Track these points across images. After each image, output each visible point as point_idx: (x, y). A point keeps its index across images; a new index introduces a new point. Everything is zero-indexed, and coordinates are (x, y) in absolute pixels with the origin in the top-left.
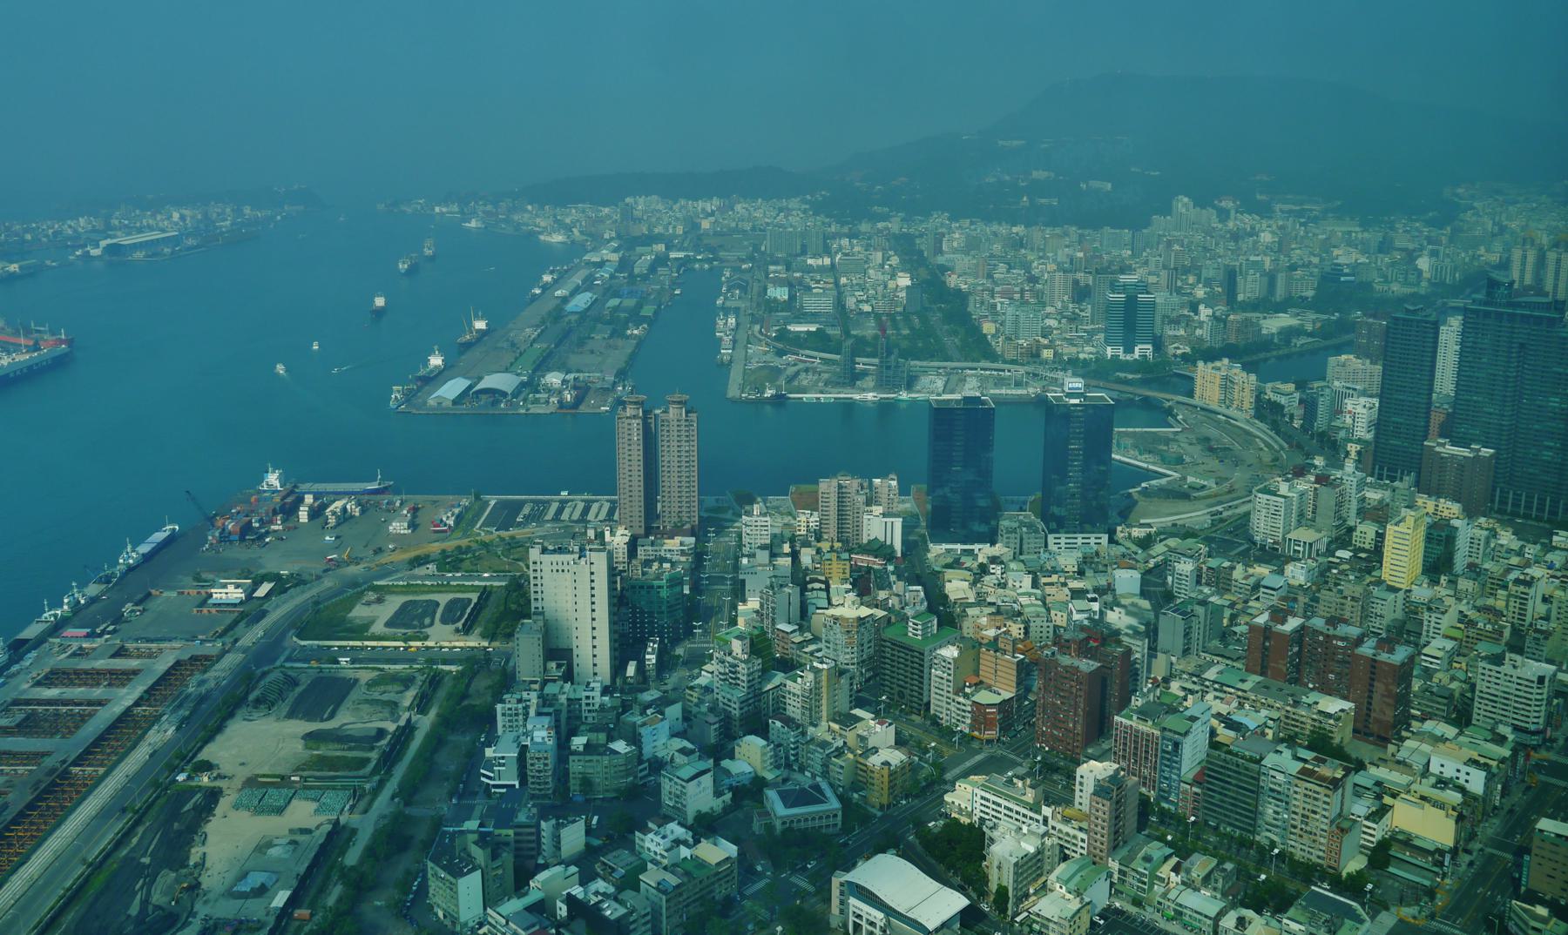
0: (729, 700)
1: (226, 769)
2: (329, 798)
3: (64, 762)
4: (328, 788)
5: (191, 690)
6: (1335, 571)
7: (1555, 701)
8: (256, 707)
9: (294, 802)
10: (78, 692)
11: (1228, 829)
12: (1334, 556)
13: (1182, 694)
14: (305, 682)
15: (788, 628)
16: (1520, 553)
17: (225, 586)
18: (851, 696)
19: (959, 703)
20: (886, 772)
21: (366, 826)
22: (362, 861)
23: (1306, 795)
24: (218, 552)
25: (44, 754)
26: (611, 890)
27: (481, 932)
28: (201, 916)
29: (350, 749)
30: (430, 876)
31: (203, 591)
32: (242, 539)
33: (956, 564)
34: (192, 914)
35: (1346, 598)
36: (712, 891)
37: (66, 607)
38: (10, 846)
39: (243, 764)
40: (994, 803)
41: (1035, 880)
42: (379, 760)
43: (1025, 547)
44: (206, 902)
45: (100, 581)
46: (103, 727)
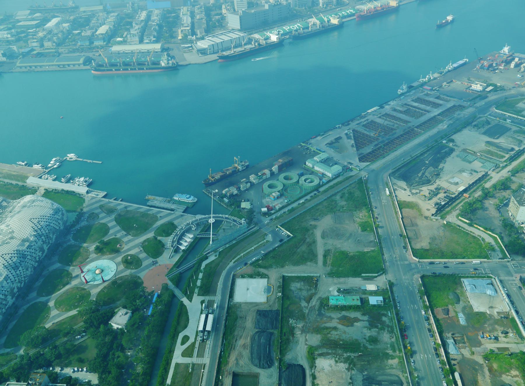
1: (458, 144)
2: (487, 164)
3: (413, 126)
4: (488, 161)
5: (455, 116)
8: (474, 127)
9: (476, 161)
10: (423, 106)
14: (493, 124)
17: (477, 84)
21: (496, 177)
22: (490, 188)
24: (478, 72)
25: (410, 122)
27: (522, 226)
28: (437, 184)
29: (500, 151)
30: (511, 201)
31: (469, 84)
32: (488, 69)
34: (435, 182)
37: (427, 79)
38: (394, 145)
39: (463, 144)
42: (508, 158)
44: (440, 180)
45: (438, 73)
46: (427, 119)
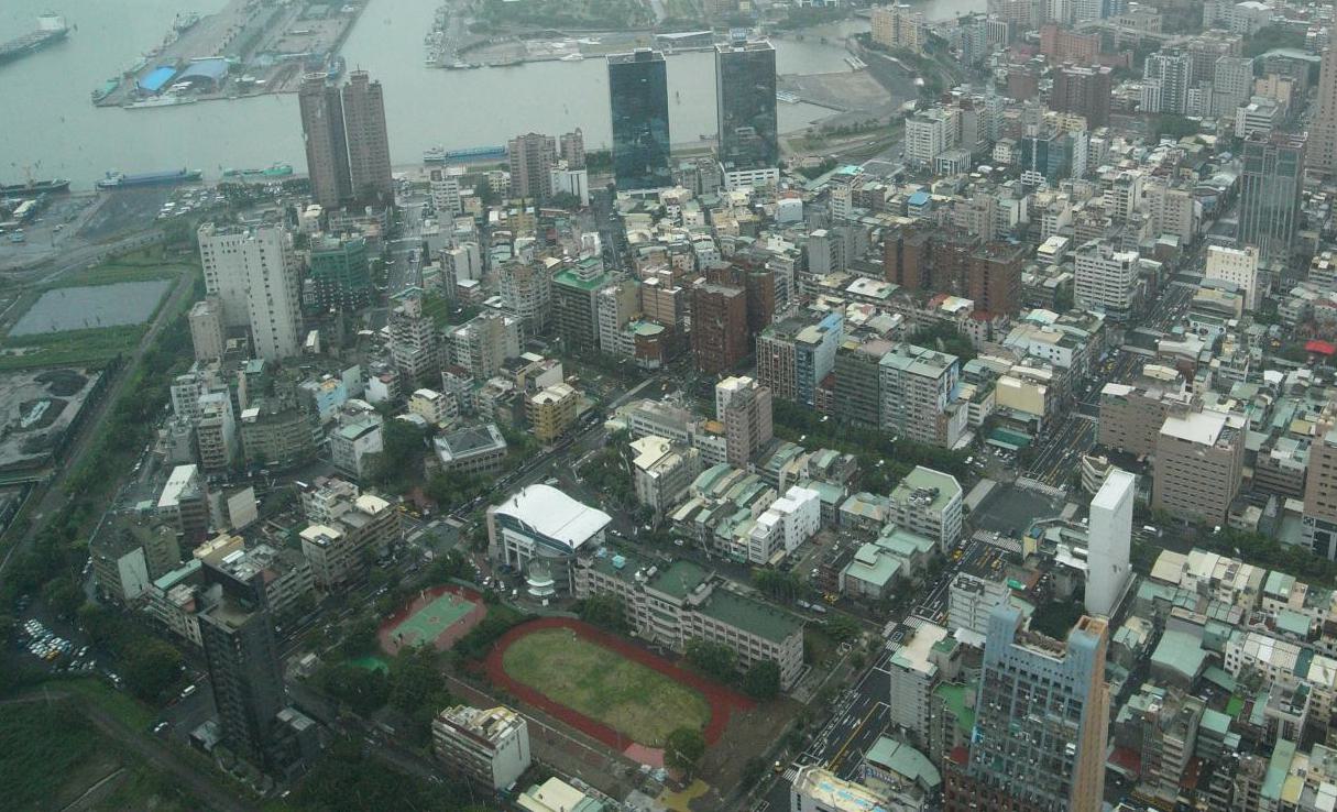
0: (404, 358)
6: (972, 185)
7: (1140, 281)
11: (860, 425)
12: (976, 172)
13: (827, 308)
15: (467, 283)
16: (1129, 156)
18: (520, 342)
20: (549, 409)
23: (916, 387)
33: (640, 209)
35: (974, 208)
40: (646, 425)
41: (679, 490)
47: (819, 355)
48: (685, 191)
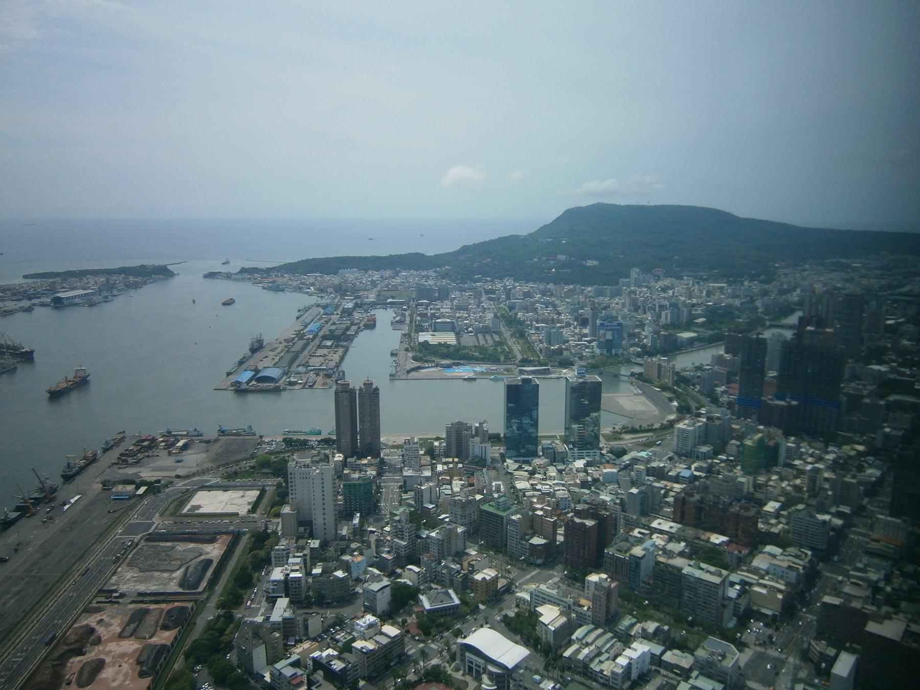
19: (522, 544)
26: (336, 653)
36: (391, 652)
40: (542, 598)
43: (557, 459)
47: (643, 564)
48: (546, 460)
